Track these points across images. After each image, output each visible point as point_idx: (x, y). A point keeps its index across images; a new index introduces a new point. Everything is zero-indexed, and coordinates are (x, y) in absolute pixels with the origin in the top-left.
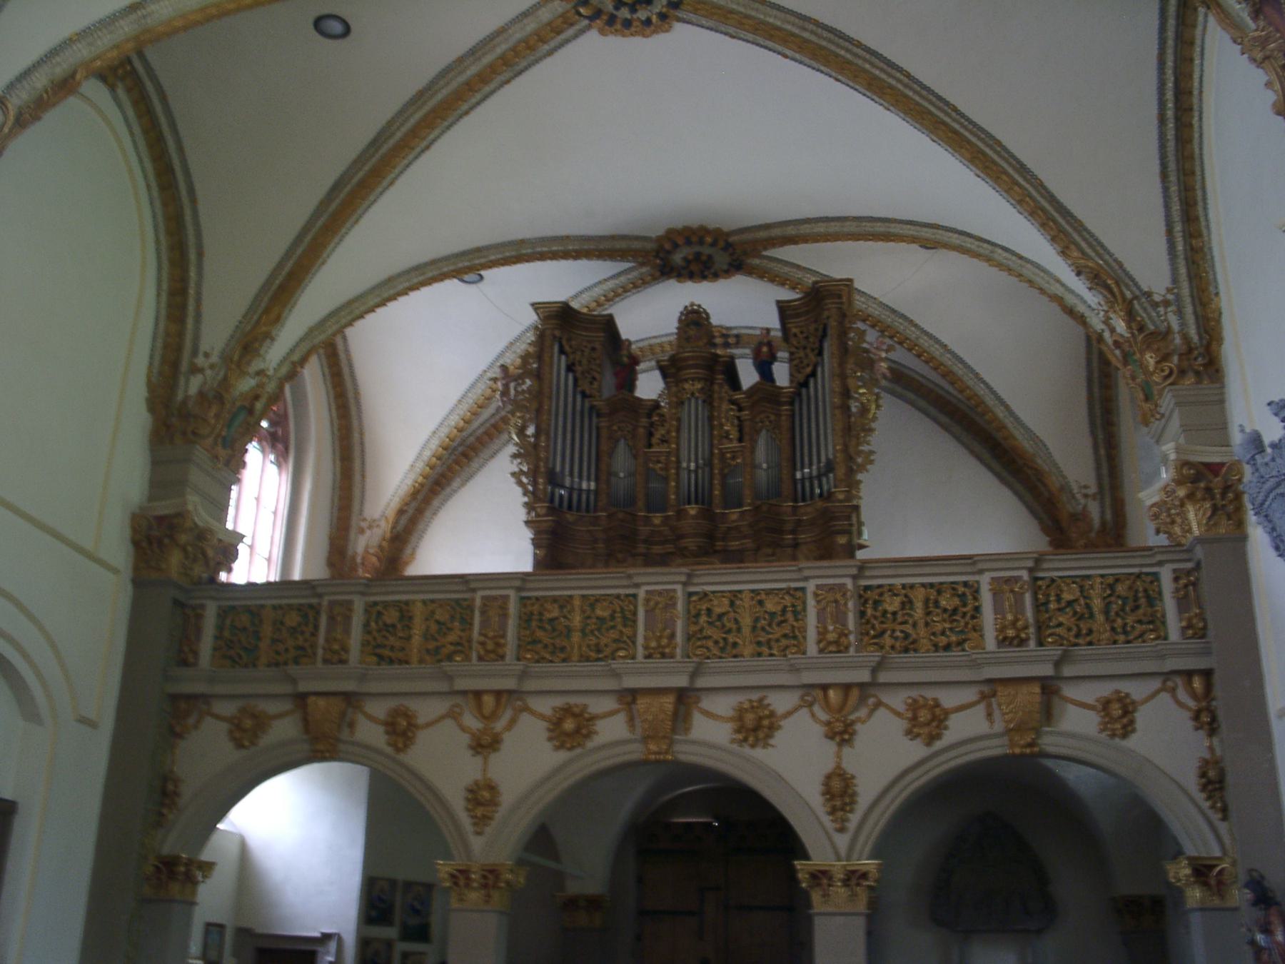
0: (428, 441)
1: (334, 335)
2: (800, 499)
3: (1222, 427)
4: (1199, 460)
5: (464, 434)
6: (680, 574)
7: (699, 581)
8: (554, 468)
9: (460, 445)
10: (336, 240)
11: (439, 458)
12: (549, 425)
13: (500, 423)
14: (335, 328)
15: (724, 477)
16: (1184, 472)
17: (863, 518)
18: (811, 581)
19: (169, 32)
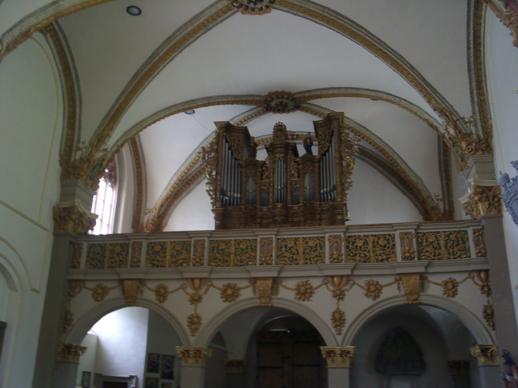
0: (173, 178)
1: (135, 135)
2: (322, 201)
3: (493, 172)
4: (483, 185)
5: (187, 175)
6: (274, 231)
7: (282, 234)
8: (223, 188)
9: (185, 179)
10: (135, 97)
11: (177, 184)
12: (221, 171)
13: (202, 170)
14: (135, 132)
15: (292, 192)
16: (477, 190)
17: (348, 208)
18: (327, 234)
19: (68, 13)
